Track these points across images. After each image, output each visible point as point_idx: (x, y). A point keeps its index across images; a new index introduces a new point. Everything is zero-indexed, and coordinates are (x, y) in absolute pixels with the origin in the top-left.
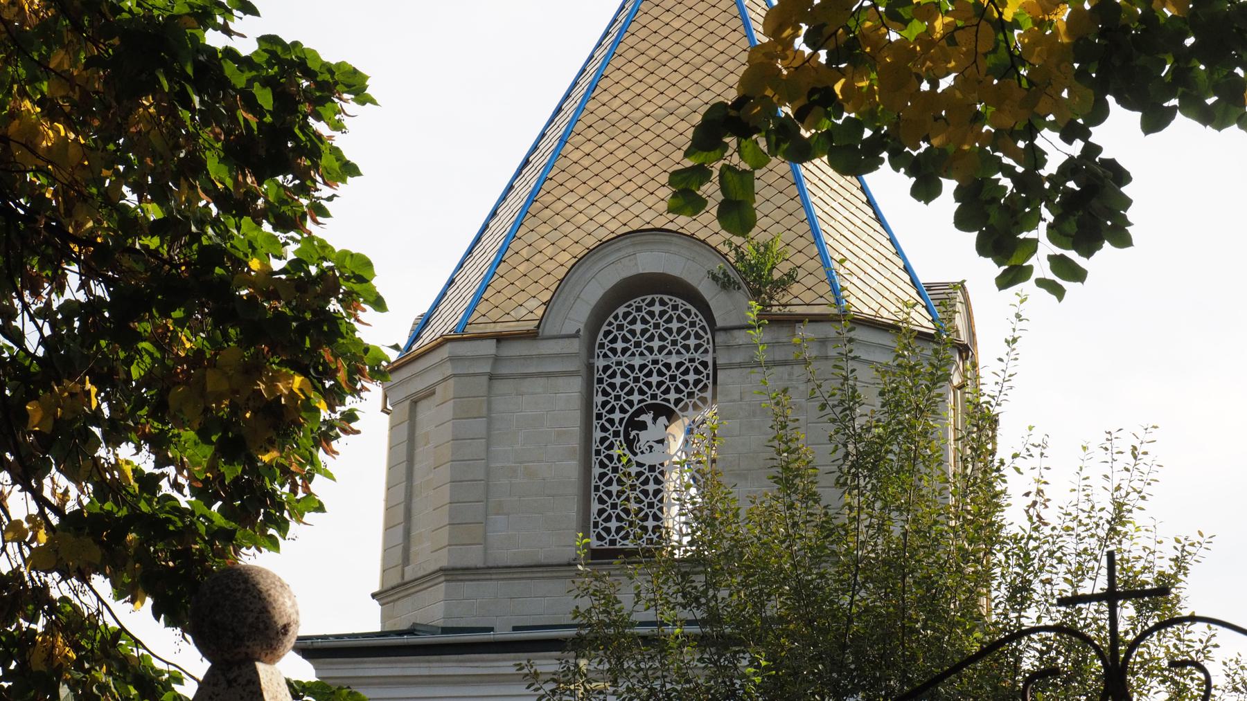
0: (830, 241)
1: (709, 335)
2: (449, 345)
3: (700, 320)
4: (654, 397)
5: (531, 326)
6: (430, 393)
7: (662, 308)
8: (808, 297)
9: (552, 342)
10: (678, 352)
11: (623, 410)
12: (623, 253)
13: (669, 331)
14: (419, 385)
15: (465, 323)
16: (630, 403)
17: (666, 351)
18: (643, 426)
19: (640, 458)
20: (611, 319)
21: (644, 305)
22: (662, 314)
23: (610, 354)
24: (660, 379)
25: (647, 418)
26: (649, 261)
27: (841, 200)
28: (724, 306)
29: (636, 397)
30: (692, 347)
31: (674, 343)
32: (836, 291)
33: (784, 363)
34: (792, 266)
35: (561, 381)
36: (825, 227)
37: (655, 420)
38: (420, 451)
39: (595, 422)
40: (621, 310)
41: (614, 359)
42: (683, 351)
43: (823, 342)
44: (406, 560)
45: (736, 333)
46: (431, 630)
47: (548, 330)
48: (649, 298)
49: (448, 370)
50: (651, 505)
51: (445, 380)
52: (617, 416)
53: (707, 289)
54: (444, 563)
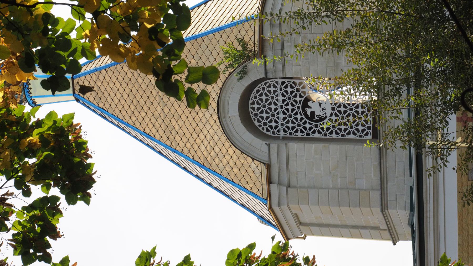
0: (224, 22)
1: (269, 81)
2: (273, 207)
3: (261, 85)
4: (298, 108)
5: (264, 167)
6: (296, 216)
7: (256, 103)
8: (251, 33)
9: (272, 157)
10: (277, 96)
11: (305, 123)
12: (228, 122)
13: (267, 100)
14: (292, 222)
15: (262, 199)
16: (301, 119)
17: (276, 102)
18: (313, 113)
19: (328, 115)
20: (261, 128)
21: (254, 113)
22: (258, 104)
23: (277, 129)
24: (290, 105)
25: (309, 111)
27: (204, 17)
29: (299, 117)
30: (274, 89)
31: (272, 98)
32: (247, 20)
33: (283, 44)
34: (236, 40)
35: (291, 153)
36: (217, 25)
37: (309, 107)
38: (324, 221)
39: (311, 136)
40: (257, 123)
41: (280, 127)
42: (276, 94)
43: (272, 26)
44: (377, 228)
45: (268, 68)
46: (411, 216)
47: (266, 159)
48: (251, 110)
49: (285, 207)
50: (351, 109)
51: (290, 209)
52: (308, 126)
53: (247, 82)
54: (379, 210)
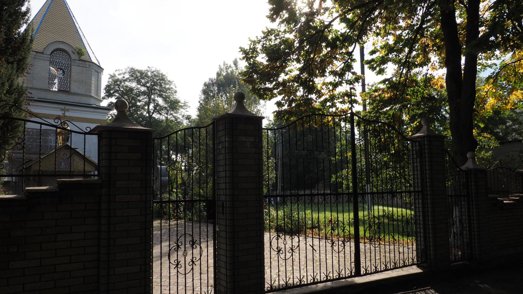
26: (61, 46)
28: (74, 57)
43: (89, 65)
53: (71, 53)
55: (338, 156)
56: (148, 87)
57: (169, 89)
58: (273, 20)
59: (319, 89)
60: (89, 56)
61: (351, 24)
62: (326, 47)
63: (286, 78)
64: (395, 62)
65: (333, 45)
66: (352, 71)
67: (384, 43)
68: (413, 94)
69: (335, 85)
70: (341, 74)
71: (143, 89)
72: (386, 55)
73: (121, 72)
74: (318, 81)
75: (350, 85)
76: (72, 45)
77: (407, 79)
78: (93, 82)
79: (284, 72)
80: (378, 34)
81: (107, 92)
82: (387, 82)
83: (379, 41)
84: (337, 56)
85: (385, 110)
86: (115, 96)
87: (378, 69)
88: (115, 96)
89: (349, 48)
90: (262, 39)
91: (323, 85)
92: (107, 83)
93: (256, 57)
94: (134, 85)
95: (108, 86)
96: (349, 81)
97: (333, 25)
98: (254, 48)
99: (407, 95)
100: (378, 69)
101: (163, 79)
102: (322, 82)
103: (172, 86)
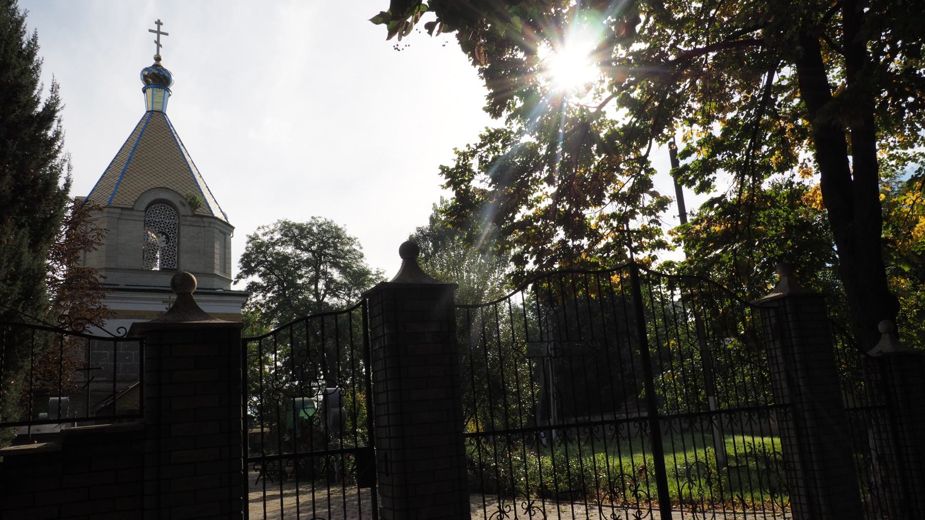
15: (110, 202)
28: (183, 210)
53: (178, 204)
55: (652, 347)
56: (313, 252)
57: (349, 251)
58: (496, 114)
59: (593, 228)
60: (209, 207)
61: (637, 108)
62: (599, 152)
63: (530, 213)
64: (729, 167)
65: (608, 146)
66: (651, 190)
67: (703, 135)
68: (769, 221)
69: (623, 218)
70: (631, 198)
71: (305, 255)
72: (709, 157)
73: (267, 230)
74: (591, 214)
75: (650, 215)
76: (180, 192)
77: (754, 195)
78: (217, 251)
79: (525, 202)
80: (691, 122)
81: (244, 266)
82: (716, 205)
83: (695, 133)
84: (621, 166)
85: (712, 255)
86: (259, 271)
87: (698, 183)
88: (259, 271)
89: (641, 150)
90: (478, 147)
91: (600, 221)
92: (244, 251)
93: (469, 181)
94: (289, 250)
95: (246, 256)
96: (646, 209)
97: (605, 113)
98: (465, 165)
99: (758, 224)
100: (698, 183)
101: (339, 237)
102: (597, 215)
103: (354, 247)
